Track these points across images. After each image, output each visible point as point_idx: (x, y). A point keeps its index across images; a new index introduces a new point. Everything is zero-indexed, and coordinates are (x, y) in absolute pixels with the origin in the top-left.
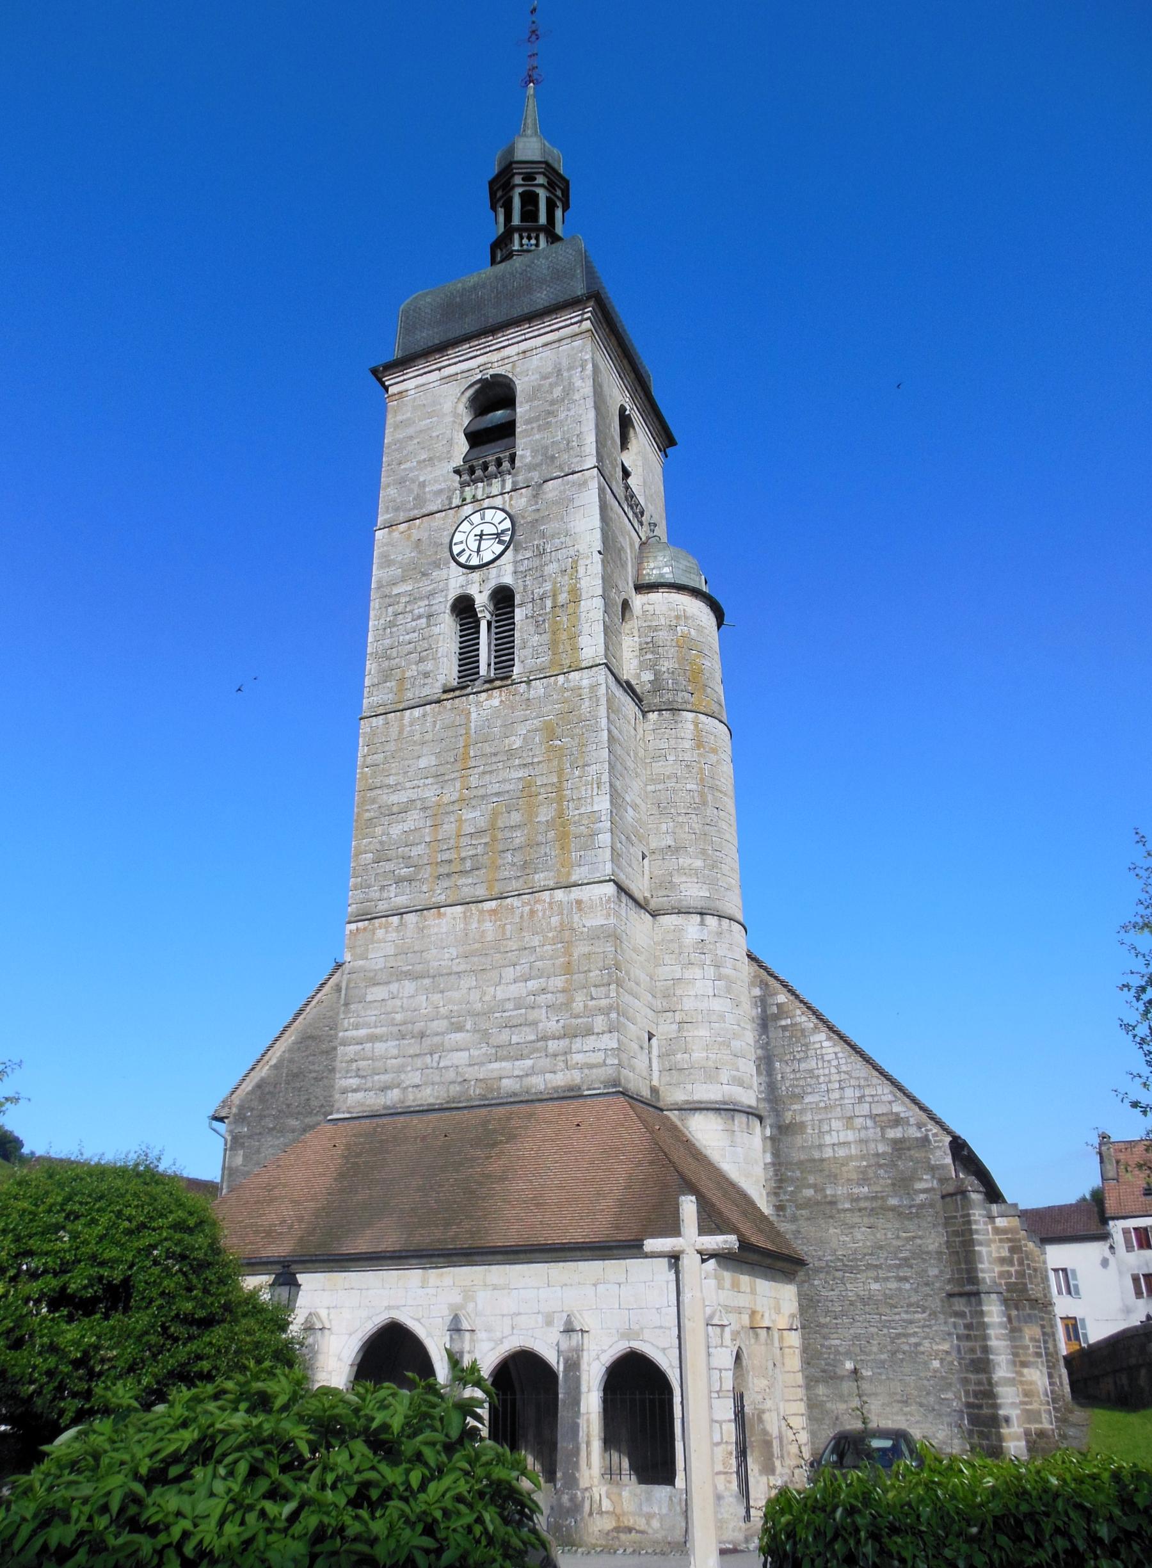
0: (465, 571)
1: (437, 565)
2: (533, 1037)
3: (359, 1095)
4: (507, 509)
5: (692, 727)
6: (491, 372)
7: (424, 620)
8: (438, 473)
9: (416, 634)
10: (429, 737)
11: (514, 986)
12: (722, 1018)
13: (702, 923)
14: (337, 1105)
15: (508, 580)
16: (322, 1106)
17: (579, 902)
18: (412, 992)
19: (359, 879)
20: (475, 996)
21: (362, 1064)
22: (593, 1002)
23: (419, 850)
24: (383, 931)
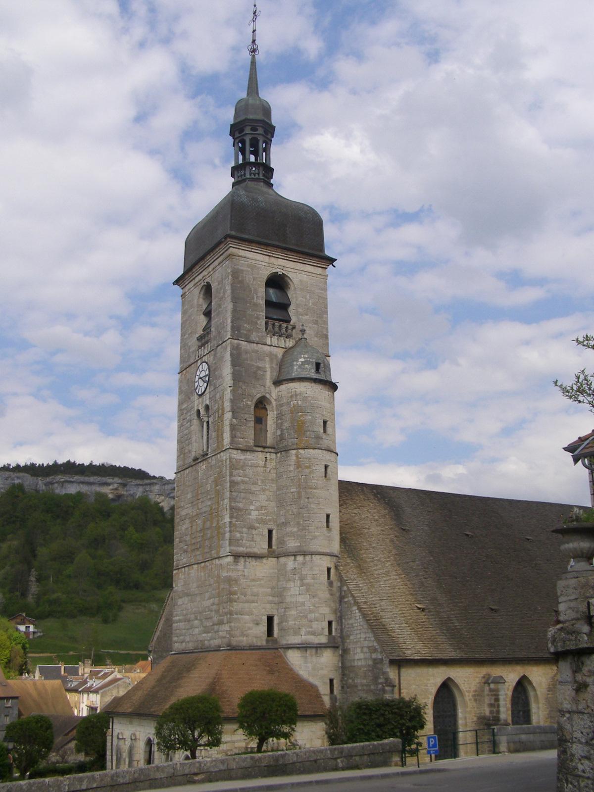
2: (211, 624)
5: (294, 458)
12: (303, 604)
13: (295, 560)
15: (208, 402)
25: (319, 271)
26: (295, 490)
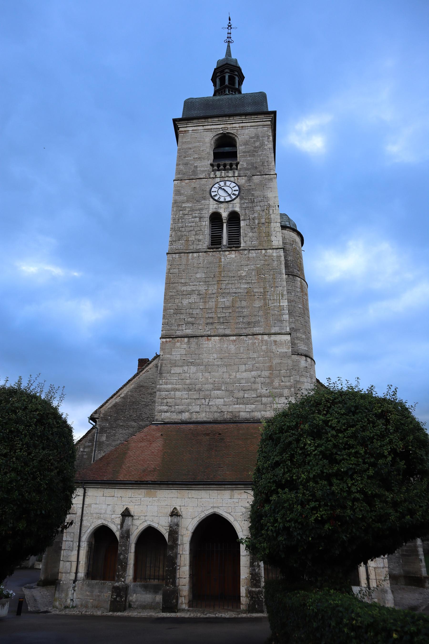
0: (217, 203)
1: (204, 198)
2: (255, 396)
3: (168, 414)
4: (236, 182)
6: (227, 131)
7: (198, 219)
8: (203, 164)
9: (194, 224)
10: (201, 265)
11: (245, 373)
13: (306, 360)
14: (156, 418)
15: (237, 209)
16: (148, 417)
17: (275, 341)
18: (194, 371)
19: (167, 320)
20: (226, 376)
21: (169, 400)
22: (283, 383)
23: (198, 311)
24: (179, 343)
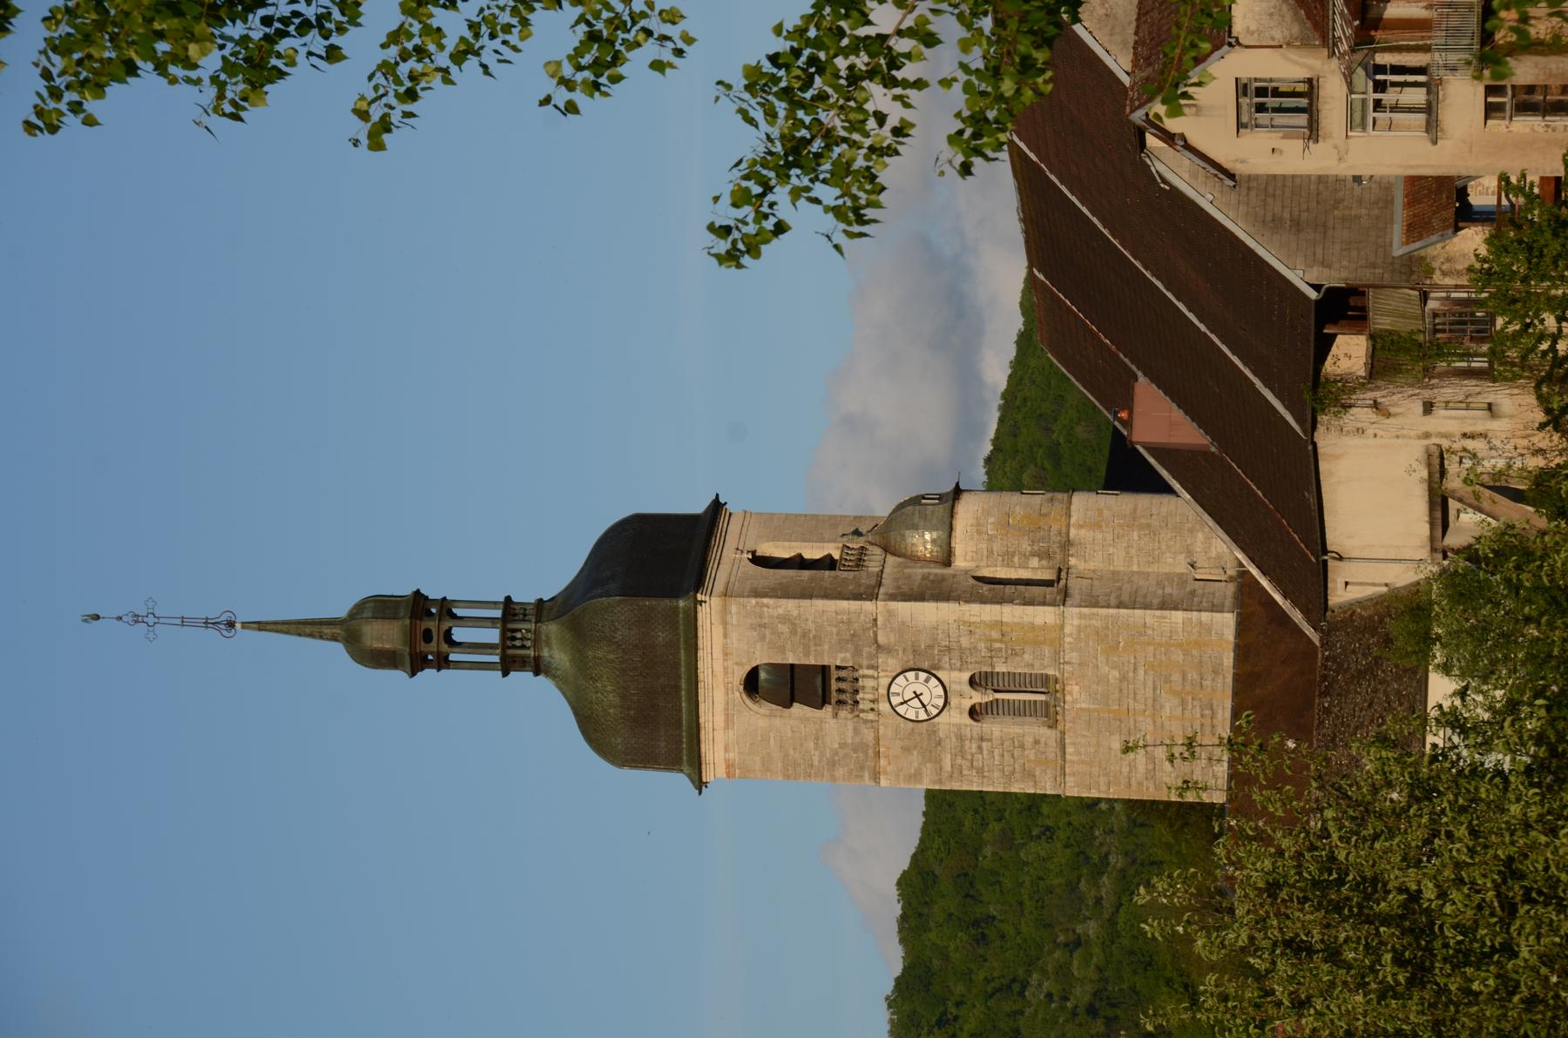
5: (1083, 532)
15: (966, 676)
25: (734, 528)
26: (1135, 534)
